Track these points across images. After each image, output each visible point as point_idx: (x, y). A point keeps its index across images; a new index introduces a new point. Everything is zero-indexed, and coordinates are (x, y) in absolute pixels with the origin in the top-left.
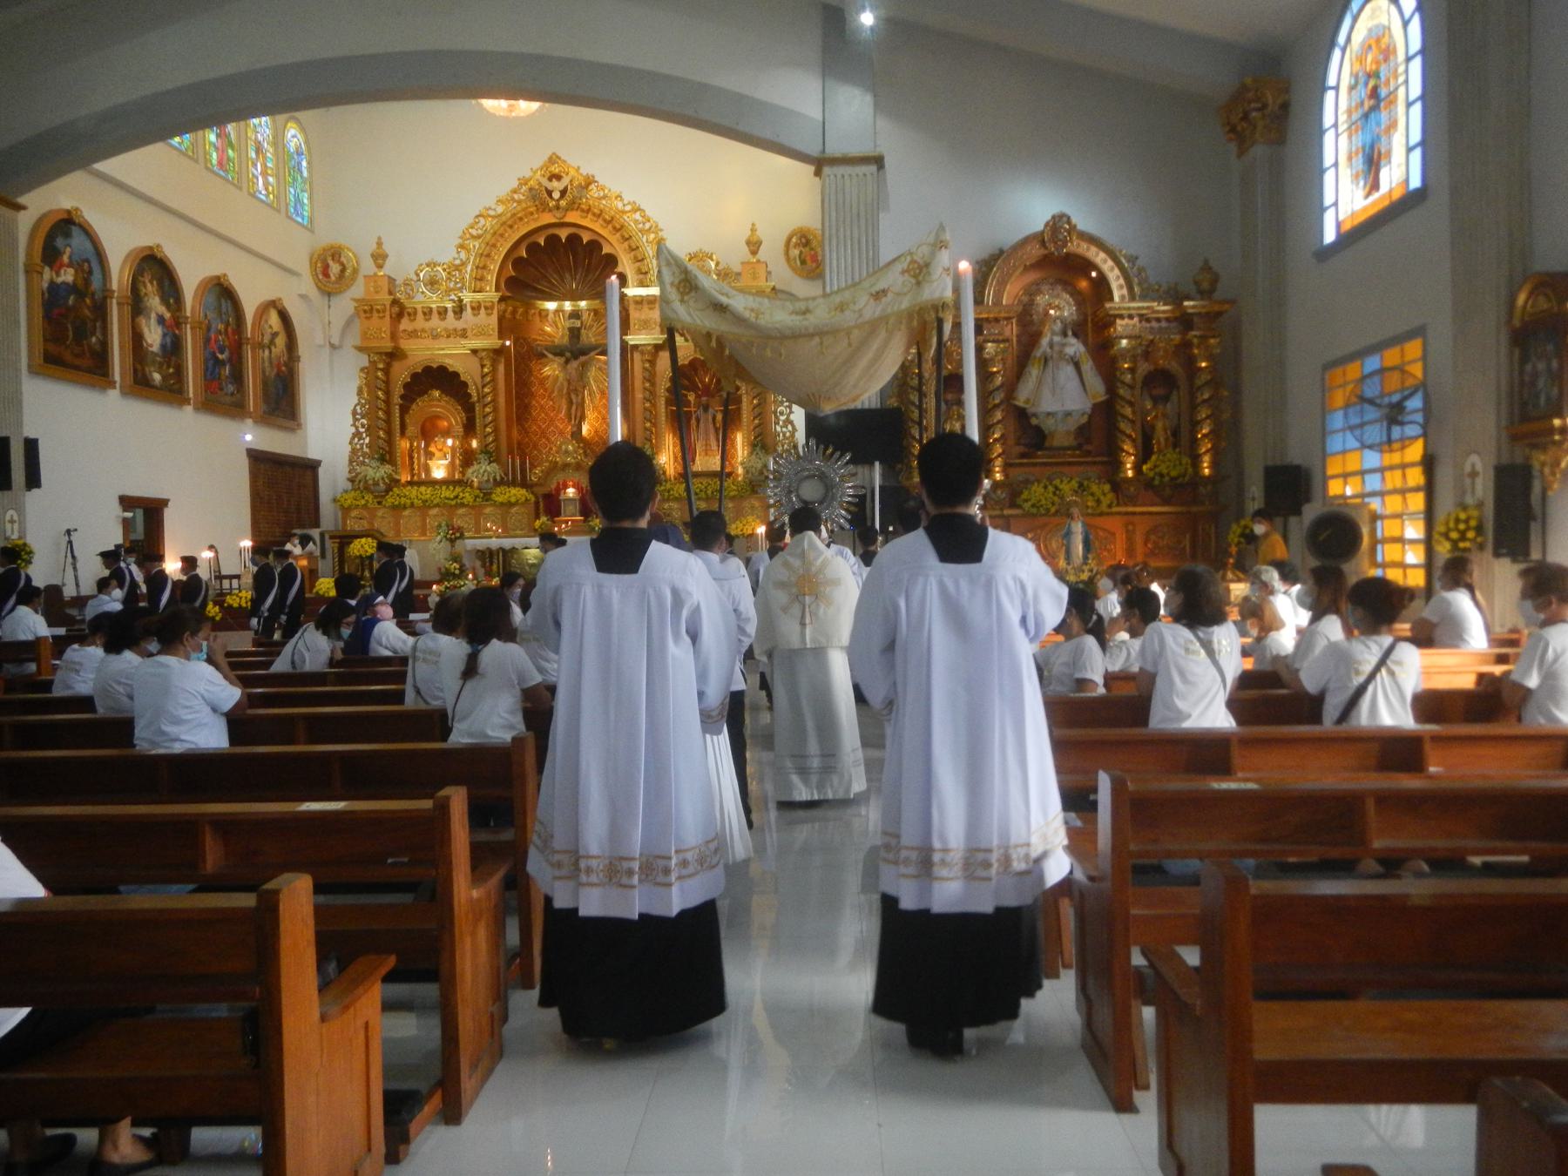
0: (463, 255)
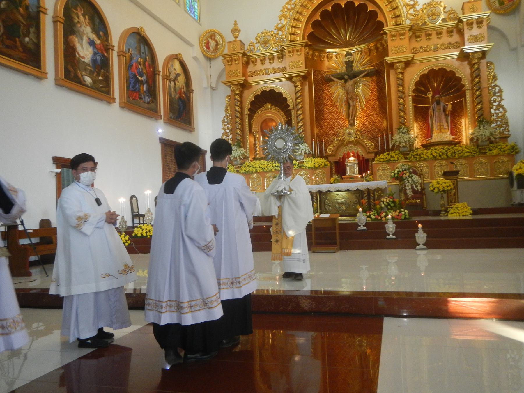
0: (283, 22)
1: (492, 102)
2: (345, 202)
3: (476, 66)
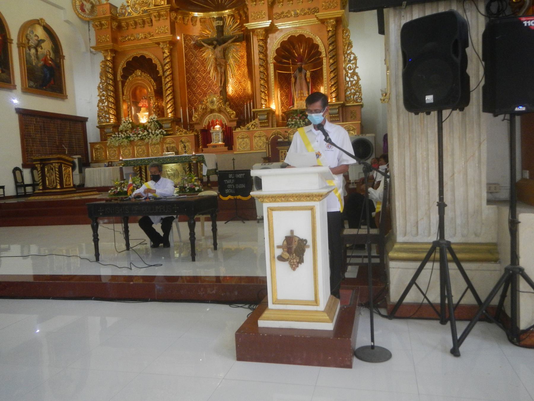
1: (347, 69)
3: (330, 34)
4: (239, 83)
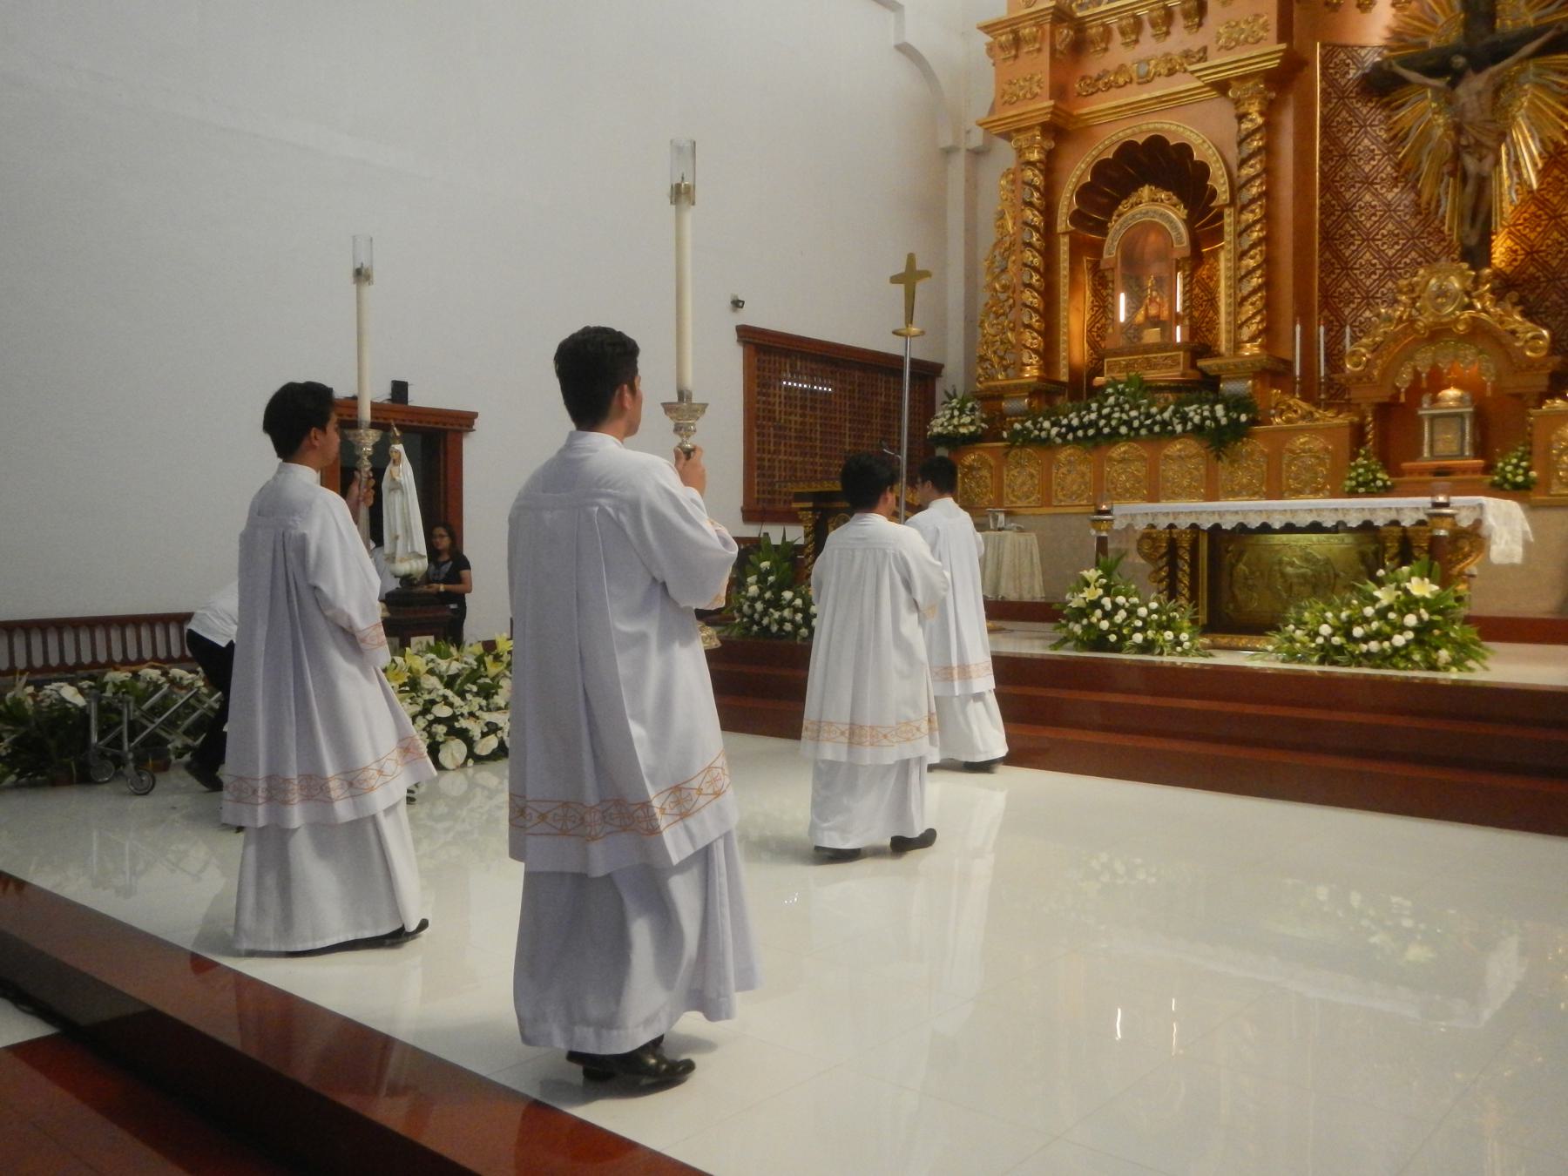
2: (1314, 576)
4: (1551, 218)
